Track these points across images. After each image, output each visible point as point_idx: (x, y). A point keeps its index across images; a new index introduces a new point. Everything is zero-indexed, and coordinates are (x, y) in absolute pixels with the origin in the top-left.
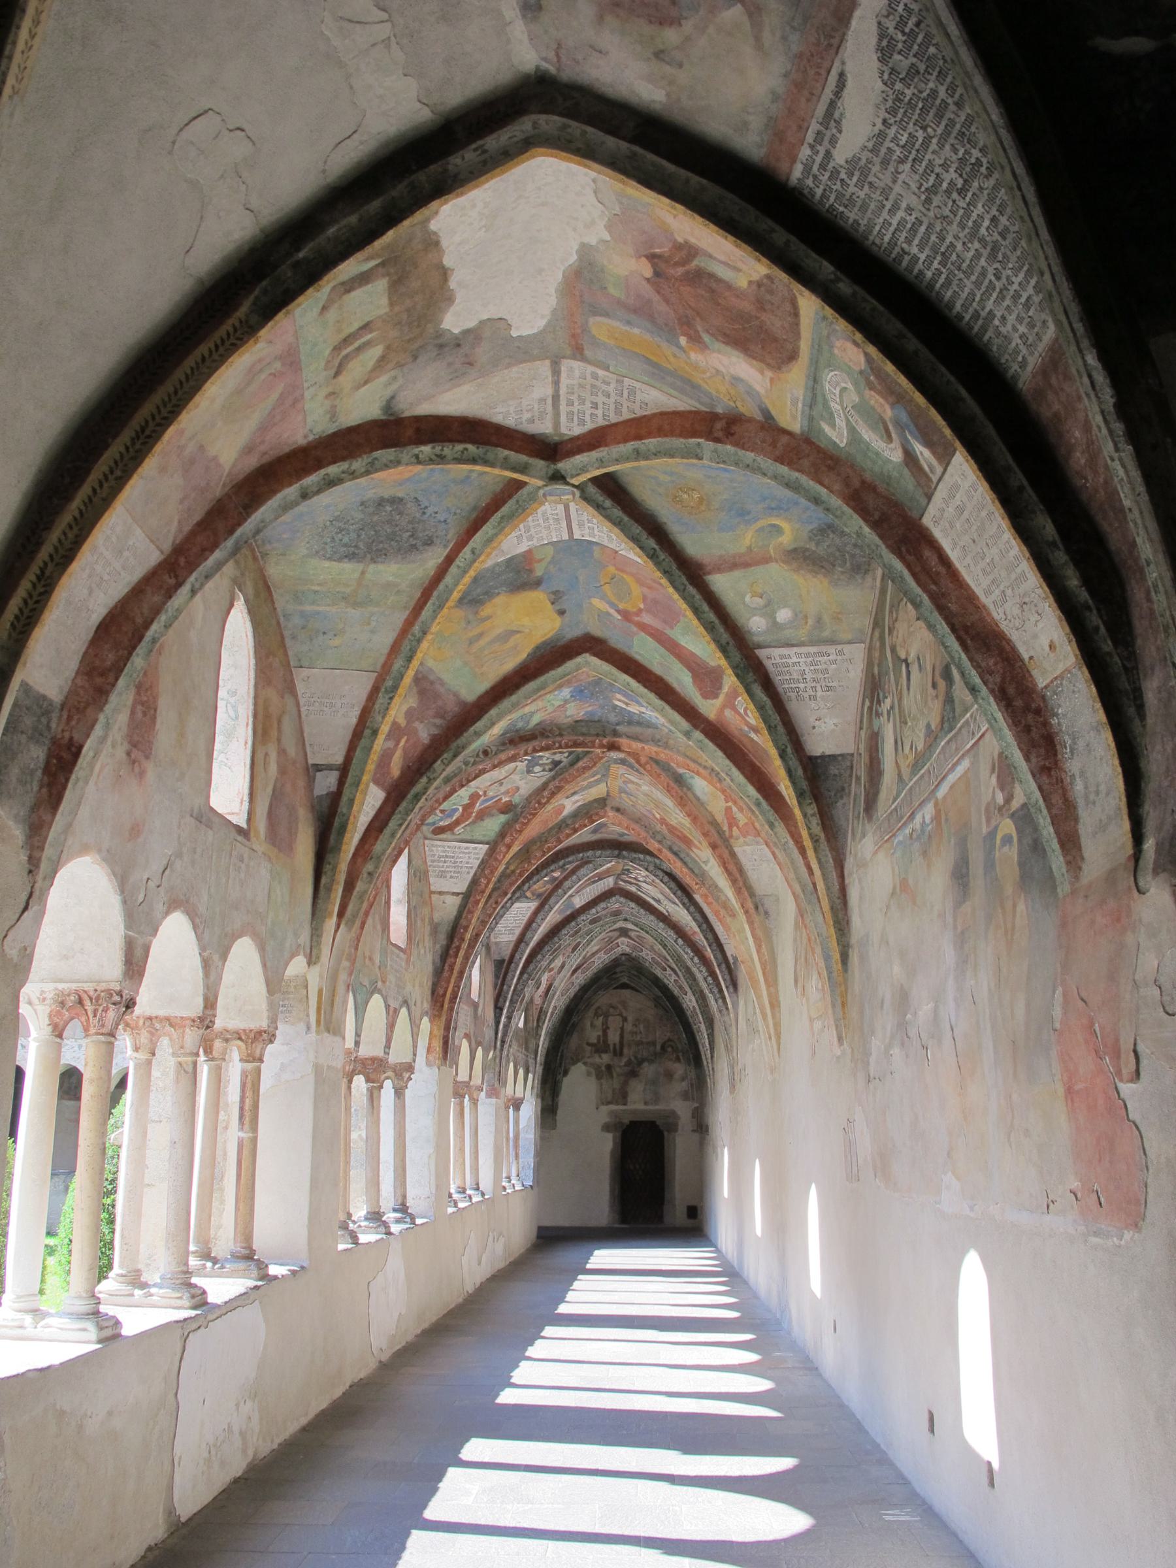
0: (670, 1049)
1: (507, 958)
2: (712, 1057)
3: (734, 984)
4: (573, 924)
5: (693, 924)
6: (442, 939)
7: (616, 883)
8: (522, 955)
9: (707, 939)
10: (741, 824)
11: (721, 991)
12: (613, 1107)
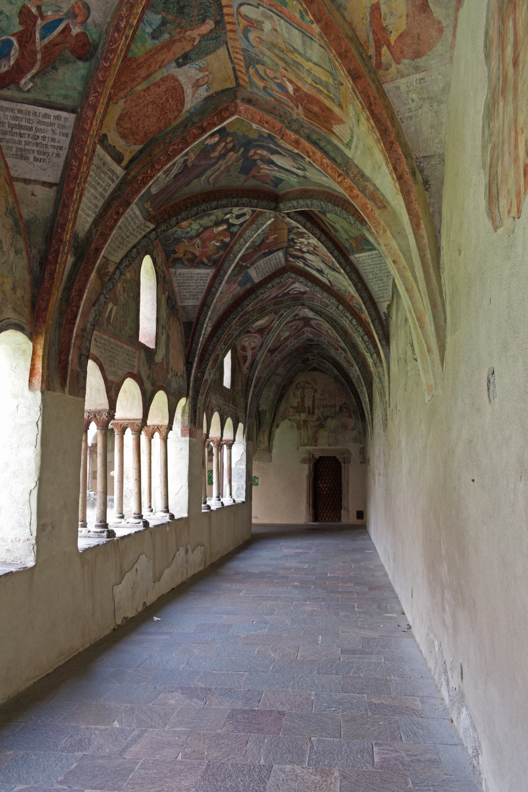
0: (345, 410)
1: (194, 321)
3: (386, 338)
4: (253, 296)
5: (352, 290)
6: (39, 239)
7: (286, 260)
8: (206, 316)
9: (362, 297)
10: (393, 39)
11: (375, 346)
12: (308, 448)
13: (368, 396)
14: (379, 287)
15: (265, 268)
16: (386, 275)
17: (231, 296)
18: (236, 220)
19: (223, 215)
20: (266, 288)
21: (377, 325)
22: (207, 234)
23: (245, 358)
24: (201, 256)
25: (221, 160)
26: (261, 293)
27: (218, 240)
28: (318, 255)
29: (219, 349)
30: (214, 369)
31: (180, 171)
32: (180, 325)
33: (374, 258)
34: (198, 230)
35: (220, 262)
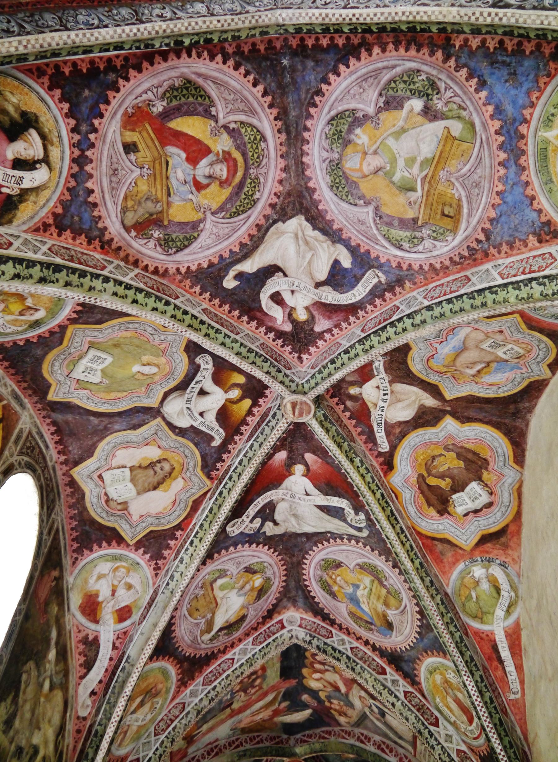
4: (125, 12)
23: (92, 645)
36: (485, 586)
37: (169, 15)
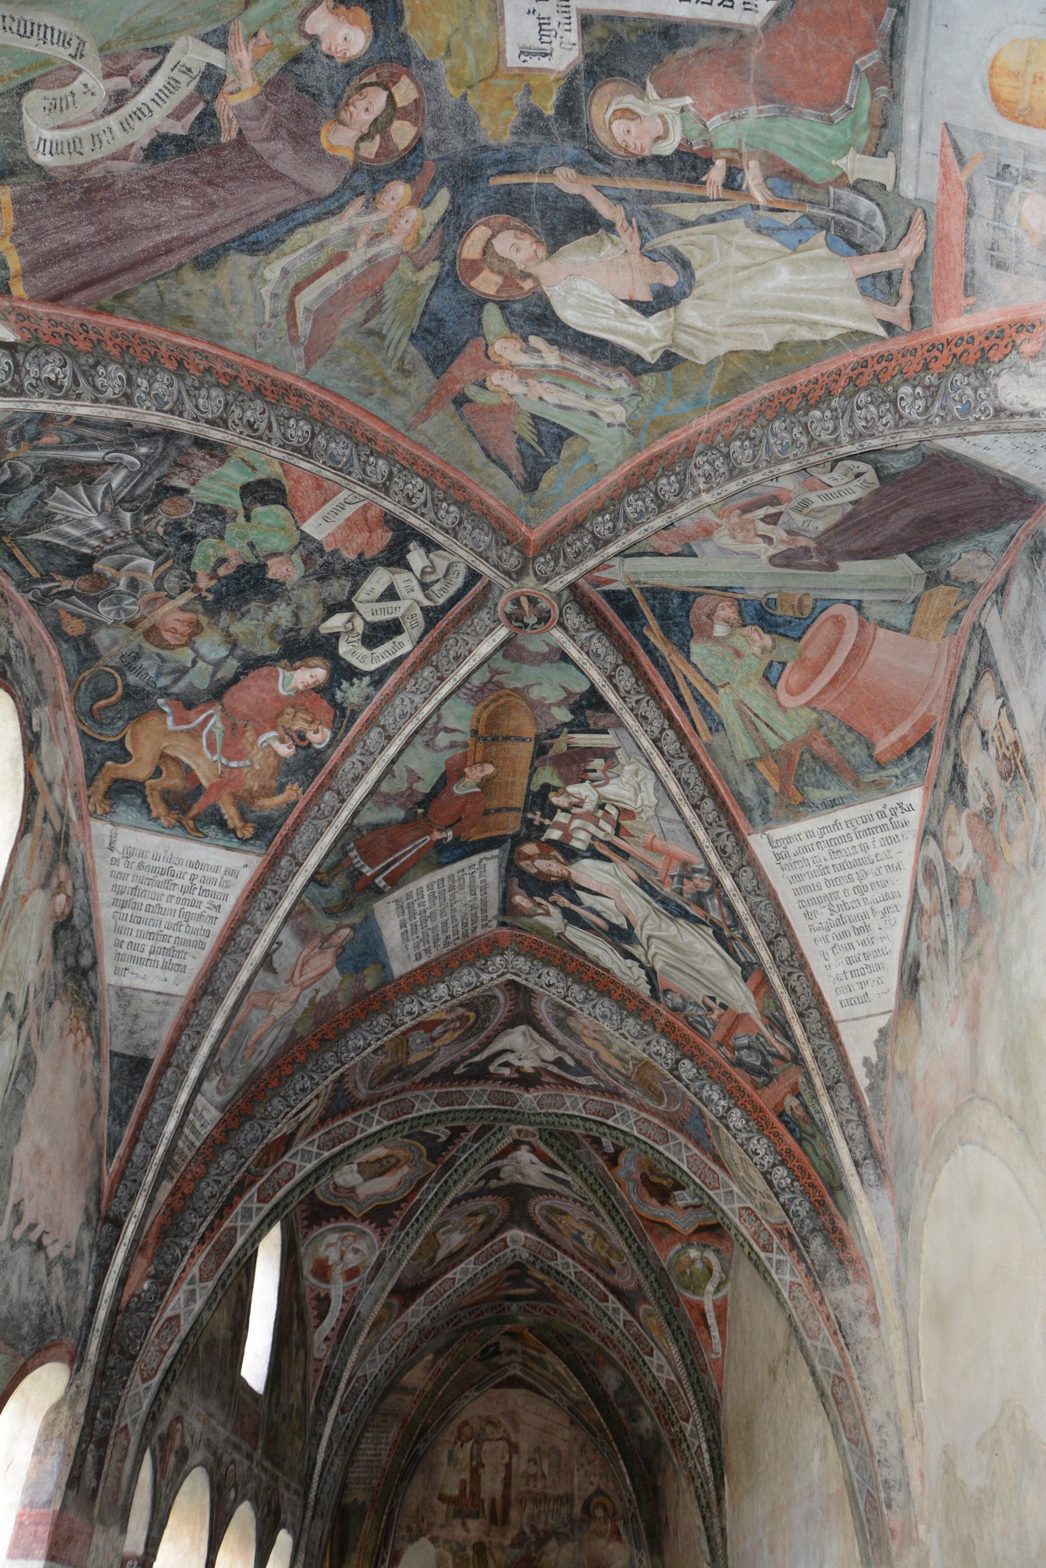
1: (157, 1056)
2: (720, 1499)
4: (382, 1019)
7: (507, 907)
13: (710, 1450)
14: (850, 961)
15: (433, 916)
16: (879, 907)
17: (304, 1003)
18: (363, 651)
19: (319, 612)
20: (428, 997)
21: (845, 1104)
22: (249, 694)
23: (324, 1302)
24: (218, 787)
25: (360, 201)
26: (410, 1013)
27: (287, 731)
28: (625, 855)
29: (238, 1208)
30: (207, 1279)
31: (179, 128)
32: (98, 1056)
33: (843, 839)
34: (218, 664)
35: (283, 831)
36: (699, 1265)
37: (416, 1009)
